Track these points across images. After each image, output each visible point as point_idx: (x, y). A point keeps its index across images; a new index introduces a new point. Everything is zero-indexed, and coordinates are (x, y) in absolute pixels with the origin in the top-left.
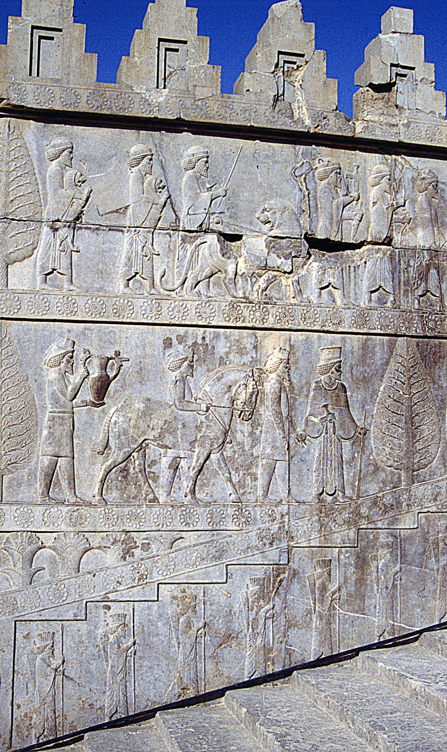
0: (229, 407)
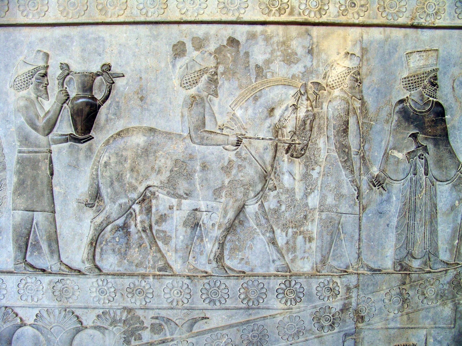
0: (271, 139)
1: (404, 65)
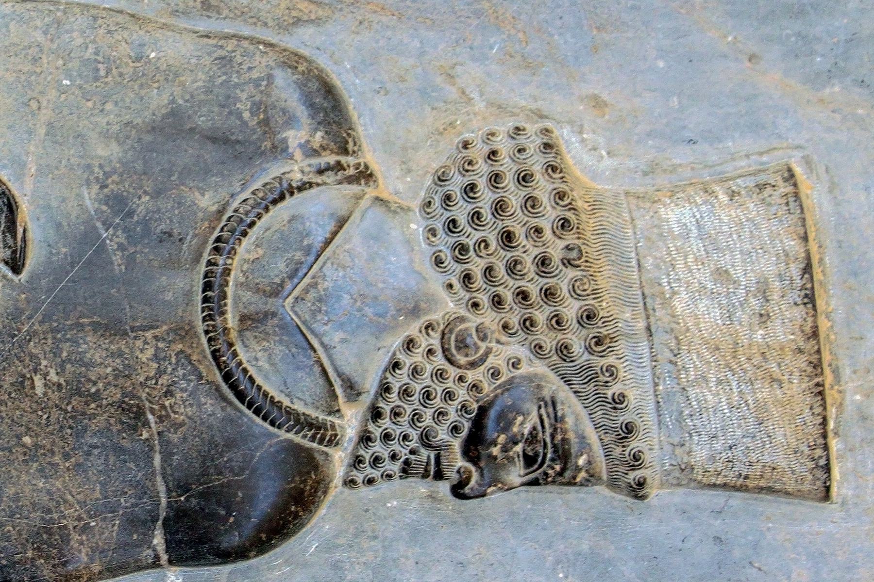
1: (681, 156)
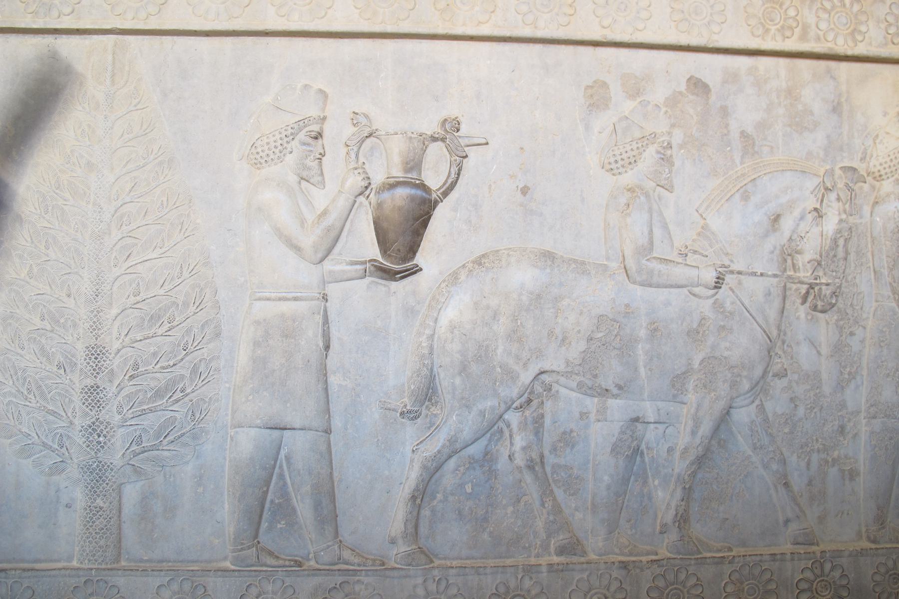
0: (775, 276)
